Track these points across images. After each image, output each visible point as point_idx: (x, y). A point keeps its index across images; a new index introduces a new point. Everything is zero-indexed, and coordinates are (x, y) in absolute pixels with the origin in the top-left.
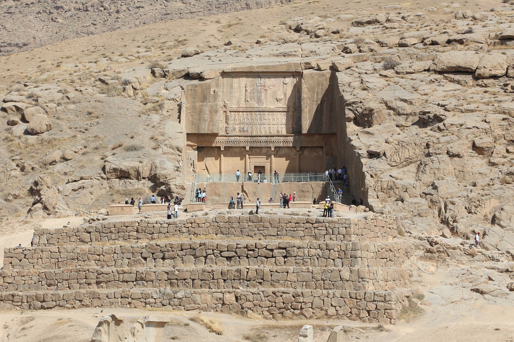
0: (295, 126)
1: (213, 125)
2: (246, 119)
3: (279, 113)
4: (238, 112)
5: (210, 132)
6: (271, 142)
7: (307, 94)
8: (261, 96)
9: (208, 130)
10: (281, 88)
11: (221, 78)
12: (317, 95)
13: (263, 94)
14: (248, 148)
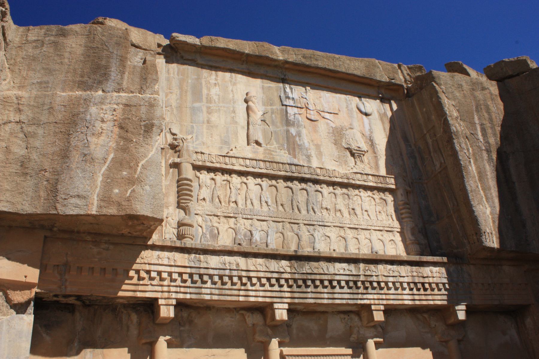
1: (131, 181)
2: (256, 202)
3: (364, 194)
4: (224, 171)
5: (112, 211)
6: (369, 285)
8: (299, 134)
9: (106, 199)
11: (161, 61)
12: (484, 135)
13: (304, 132)
14: (281, 313)
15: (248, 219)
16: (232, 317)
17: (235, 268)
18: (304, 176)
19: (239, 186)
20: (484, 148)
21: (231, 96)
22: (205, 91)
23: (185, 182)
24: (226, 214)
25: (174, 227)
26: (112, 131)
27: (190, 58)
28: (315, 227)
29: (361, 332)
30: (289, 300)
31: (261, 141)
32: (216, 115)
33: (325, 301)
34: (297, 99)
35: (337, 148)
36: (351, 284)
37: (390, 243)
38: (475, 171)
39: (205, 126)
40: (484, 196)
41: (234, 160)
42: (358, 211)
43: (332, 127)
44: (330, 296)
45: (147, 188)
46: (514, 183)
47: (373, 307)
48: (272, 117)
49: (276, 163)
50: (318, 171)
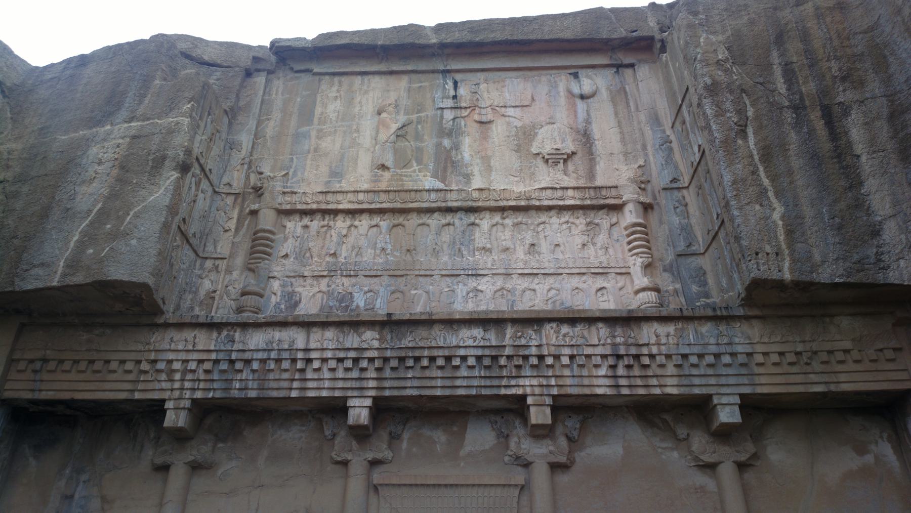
0: (668, 283)
4: (325, 212)
7: (726, 71)
8: (457, 147)
10: (562, 116)
15: (350, 276)
16: (303, 425)
17: (286, 347)
18: (450, 204)
19: (344, 232)
20: (787, 104)
21: (357, 109)
22: (318, 110)
23: (260, 235)
24: (316, 273)
25: (233, 297)
26: (108, 175)
27: (302, 67)
28: (459, 279)
29: (523, 446)
30: (373, 393)
31: (389, 164)
32: (329, 139)
33: (438, 392)
34: (461, 96)
35: (521, 157)
36: (487, 362)
37: (599, 294)
38: (752, 146)
39: (310, 156)
40: (770, 188)
41: (340, 197)
42: (544, 247)
43: (516, 127)
44: (448, 383)
45: (134, 242)
46: (858, 156)
47: (530, 400)
48: (417, 128)
49: (406, 191)
50: (475, 195)
